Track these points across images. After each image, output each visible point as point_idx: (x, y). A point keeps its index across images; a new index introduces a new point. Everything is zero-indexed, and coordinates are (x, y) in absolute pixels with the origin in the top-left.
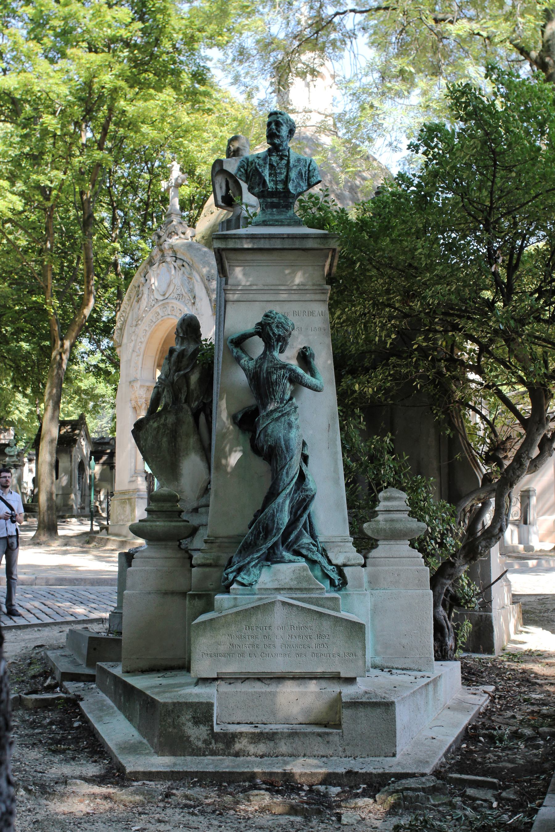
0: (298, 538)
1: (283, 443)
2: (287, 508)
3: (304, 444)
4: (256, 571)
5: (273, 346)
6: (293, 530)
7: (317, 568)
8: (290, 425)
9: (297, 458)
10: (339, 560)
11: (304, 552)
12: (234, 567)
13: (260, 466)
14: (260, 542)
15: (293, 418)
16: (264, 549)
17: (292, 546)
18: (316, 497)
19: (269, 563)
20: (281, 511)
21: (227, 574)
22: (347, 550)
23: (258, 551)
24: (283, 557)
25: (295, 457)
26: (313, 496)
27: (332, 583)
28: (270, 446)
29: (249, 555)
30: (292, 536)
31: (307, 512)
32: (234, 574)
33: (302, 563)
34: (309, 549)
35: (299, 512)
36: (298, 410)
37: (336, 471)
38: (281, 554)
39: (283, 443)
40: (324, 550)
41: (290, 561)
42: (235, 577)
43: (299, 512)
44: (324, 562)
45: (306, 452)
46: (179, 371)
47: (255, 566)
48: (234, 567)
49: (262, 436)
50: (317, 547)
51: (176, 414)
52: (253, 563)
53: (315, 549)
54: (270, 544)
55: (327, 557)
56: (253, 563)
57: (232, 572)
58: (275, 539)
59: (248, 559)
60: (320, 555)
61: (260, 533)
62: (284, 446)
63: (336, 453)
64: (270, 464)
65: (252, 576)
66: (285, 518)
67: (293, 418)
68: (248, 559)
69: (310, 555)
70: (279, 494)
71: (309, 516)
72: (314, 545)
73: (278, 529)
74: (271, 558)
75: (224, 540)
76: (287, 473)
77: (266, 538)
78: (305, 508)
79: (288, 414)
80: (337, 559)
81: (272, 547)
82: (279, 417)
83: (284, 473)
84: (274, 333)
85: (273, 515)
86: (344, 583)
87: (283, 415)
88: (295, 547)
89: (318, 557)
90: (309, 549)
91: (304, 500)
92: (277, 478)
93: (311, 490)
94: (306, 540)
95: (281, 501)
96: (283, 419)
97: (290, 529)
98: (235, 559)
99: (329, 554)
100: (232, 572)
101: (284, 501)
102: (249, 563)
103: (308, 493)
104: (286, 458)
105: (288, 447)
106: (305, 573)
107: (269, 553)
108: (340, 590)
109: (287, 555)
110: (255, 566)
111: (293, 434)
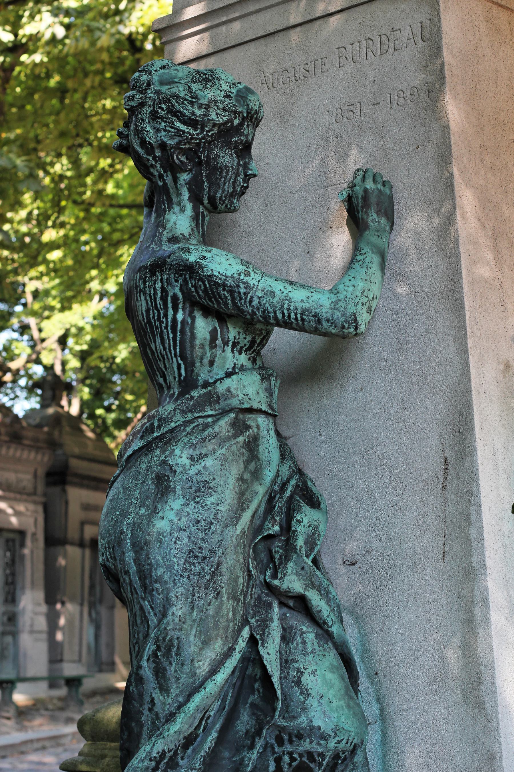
1: (129, 556)
5: (165, 189)
39: (129, 556)
67: (180, 456)
76: (160, 673)
84: (143, 143)
87: (147, 448)
103: (306, 745)
104: (146, 620)
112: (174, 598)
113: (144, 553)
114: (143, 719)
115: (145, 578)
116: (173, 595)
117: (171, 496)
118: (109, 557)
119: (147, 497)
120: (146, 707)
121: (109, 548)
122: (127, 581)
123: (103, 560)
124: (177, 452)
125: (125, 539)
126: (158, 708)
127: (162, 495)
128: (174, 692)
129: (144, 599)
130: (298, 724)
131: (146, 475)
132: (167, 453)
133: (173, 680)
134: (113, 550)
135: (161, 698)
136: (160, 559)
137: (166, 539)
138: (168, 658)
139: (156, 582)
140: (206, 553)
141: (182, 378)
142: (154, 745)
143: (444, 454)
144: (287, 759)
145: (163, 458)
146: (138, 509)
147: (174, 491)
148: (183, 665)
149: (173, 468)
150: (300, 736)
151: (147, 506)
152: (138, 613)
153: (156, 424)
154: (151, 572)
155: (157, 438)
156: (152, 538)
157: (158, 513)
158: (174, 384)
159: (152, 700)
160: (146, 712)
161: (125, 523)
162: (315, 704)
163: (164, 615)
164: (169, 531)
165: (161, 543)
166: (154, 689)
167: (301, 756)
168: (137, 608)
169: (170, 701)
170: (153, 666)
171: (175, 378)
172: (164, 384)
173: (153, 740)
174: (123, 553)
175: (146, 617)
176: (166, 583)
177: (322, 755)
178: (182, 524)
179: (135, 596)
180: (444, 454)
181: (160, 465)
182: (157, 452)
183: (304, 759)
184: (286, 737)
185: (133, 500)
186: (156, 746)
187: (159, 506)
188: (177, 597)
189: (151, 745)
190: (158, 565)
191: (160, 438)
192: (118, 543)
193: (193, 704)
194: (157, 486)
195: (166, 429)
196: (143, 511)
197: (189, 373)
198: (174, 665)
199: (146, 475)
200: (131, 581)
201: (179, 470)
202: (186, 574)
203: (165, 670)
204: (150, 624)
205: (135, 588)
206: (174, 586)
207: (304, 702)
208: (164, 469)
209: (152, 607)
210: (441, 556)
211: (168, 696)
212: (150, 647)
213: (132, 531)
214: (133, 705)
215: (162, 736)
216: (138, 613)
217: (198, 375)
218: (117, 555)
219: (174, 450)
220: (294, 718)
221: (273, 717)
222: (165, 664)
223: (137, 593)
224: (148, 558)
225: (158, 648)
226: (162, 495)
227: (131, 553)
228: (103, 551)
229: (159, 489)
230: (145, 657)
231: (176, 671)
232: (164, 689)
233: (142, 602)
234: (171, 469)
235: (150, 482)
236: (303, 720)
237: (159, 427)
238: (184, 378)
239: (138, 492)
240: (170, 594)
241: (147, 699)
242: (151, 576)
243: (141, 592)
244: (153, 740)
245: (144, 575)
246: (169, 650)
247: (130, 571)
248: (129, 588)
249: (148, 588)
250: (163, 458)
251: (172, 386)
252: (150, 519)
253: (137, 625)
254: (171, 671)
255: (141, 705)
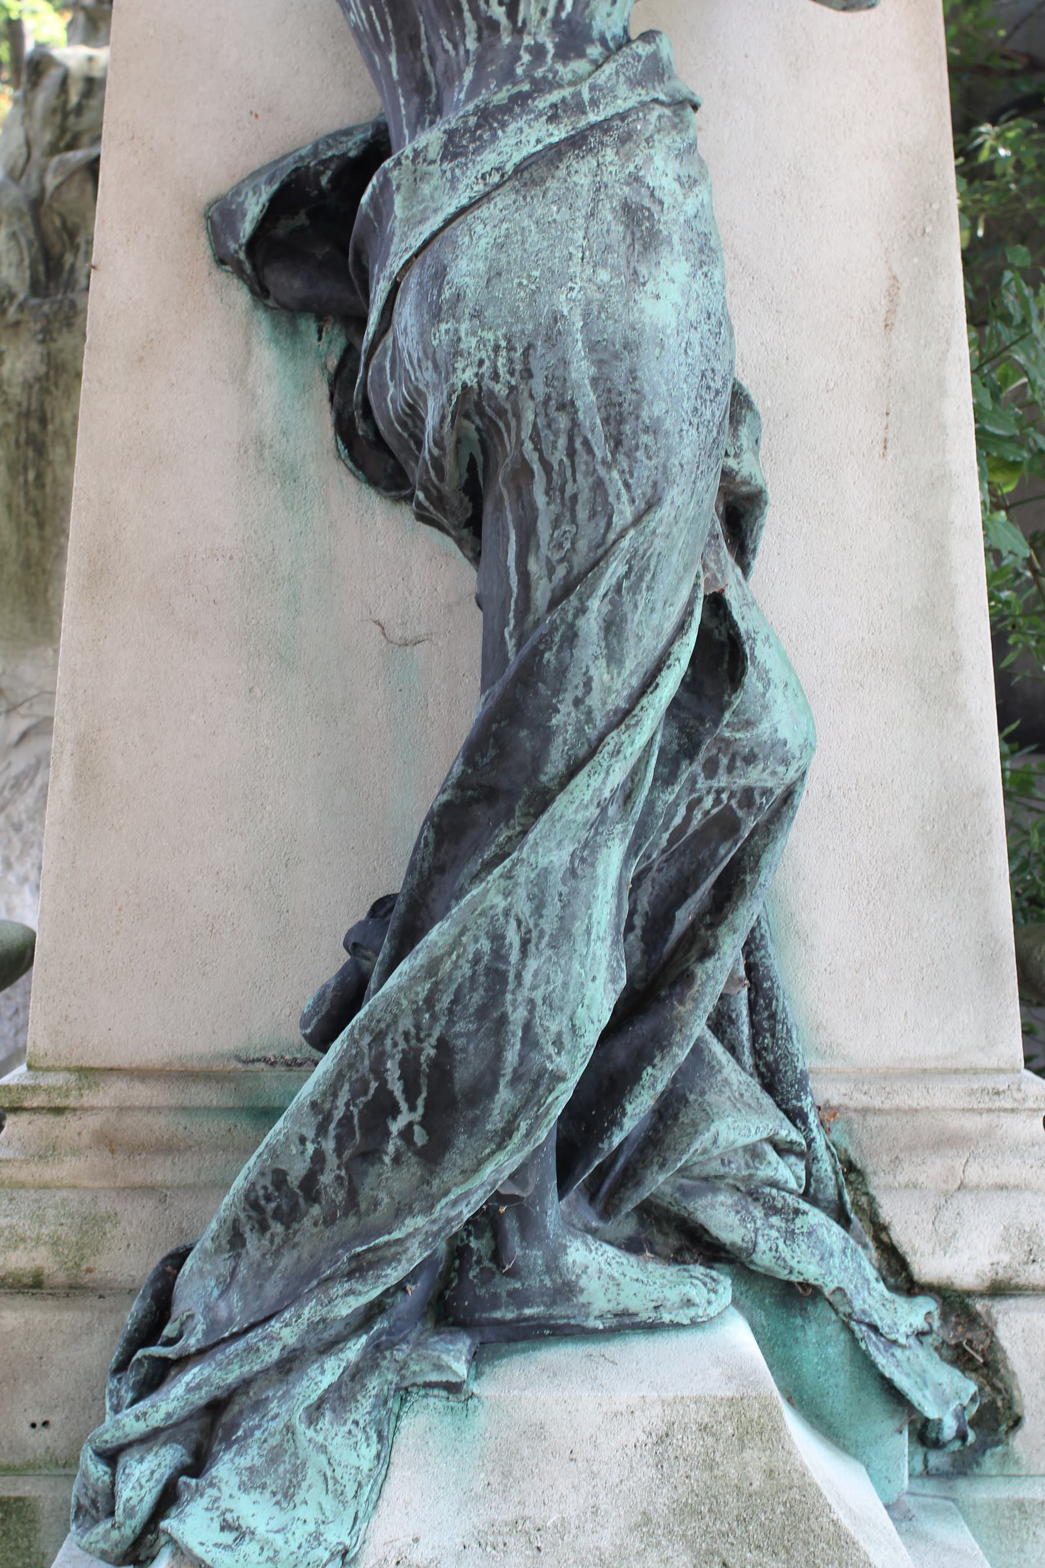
0: (669, 1109)
1: (581, 369)
2: (603, 907)
3: (740, 402)
4: (344, 1446)
6: (643, 1058)
7: (820, 1344)
8: (640, 223)
9: (688, 508)
10: (957, 1254)
11: (722, 1218)
12: (175, 1398)
13: (404, 569)
14: (390, 1180)
15: (661, 170)
16: (415, 1242)
17: (631, 1176)
18: (805, 803)
19: (455, 1358)
20: (563, 935)
21: (111, 1457)
22: (1011, 1170)
23: (360, 1269)
24: (566, 1290)
25: (675, 496)
26: (788, 796)
27: (924, 1434)
28: (471, 404)
29: (292, 1298)
30: (638, 1109)
31: (744, 916)
32: (165, 1459)
33: (727, 1344)
34: (753, 1193)
35: (684, 917)
36: (695, 118)
37: (934, 613)
38: (553, 1266)
39: (581, 369)
40: (851, 1170)
41: (625, 1325)
42: (168, 1499)
43: (684, 917)
44: (872, 1297)
45: (746, 467)
46: (71, 146)
47: (338, 1398)
48: (175, 1398)
49: (406, 314)
50: (807, 1155)
51: (46, 336)
52: (327, 1373)
53: (788, 1172)
54: (464, 1199)
55: (879, 1230)
56: (327, 1373)
57: (150, 1438)
58: (498, 1169)
59: (286, 1332)
60: (833, 1233)
61: (382, 1108)
62: (587, 399)
63: (939, 482)
64: (476, 558)
65: (313, 1495)
66: (593, 985)
68: (286, 1332)
69: (767, 1245)
70: (542, 801)
71: (752, 947)
72: (783, 1149)
73: (535, 1082)
74: (477, 1301)
75: (142, 1093)
76: (613, 626)
77: (432, 1155)
78: (730, 889)
79: (620, 131)
80: (946, 1243)
81: (487, 1220)
82: (553, 155)
83: (591, 625)
85: (496, 976)
86: (995, 1418)
87: (577, 142)
88: (658, 1182)
89: (826, 1255)
90: (753, 1193)
91: (724, 824)
92: (530, 673)
93: (778, 751)
94: (737, 1121)
95: (559, 858)
96: (581, 172)
97: (620, 1052)
98: (195, 1293)
99: (889, 1210)
100: (150, 1438)
101: (585, 856)
102: (289, 1365)
103: (755, 776)
105: (617, 417)
106: (754, 1457)
107: (459, 1251)
108: (965, 1464)
109: (599, 1268)
110: (338, 1398)
111: (666, 300)
112: (676, 470)
113: (623, 367)
114: (554, 721)
115: (621, 421)
116: (677, 463)
117: (664, 250)
118: (502, 371)
119: (608, 248)
120: (569, 697)
121: (511, 348)
122: (563, 422)
123: (477, 375)
124: (658, 161)
125: (569, 333)
126: (594, 700)
127: (646, 247)
128: (630, 665)
129: (607, 465)
130: (758, 736)
131: (596, 201)
132: (638, 161)
133: (632, 641)
134: (526, 354)
135: (606, 677)
136: (662, 382)
137: (671, 341)
138: (634, 594)
139: (646, 430)
140: (719, 384)
141: (564, 15)
142: (607, 773)
143: (890, 269)
144: (708, 802)
145: (631, 168)
146: (589, 271)
147: (670, 243)
148: (652, 610)
149: (656, 193)
150: (750, 759)
151: (613, 268)
152: (585, 496)
153: (586, 96)
154: (638, 406)
155: (592, 127)
156: (641, 335)
157: (644, 284)
158: (539, 25)
159: (588, 685)
160: (566, 707)
161: (563, 298)
162: (780, 699)
163: (652, 504)
164: (674, 325)
165: (663, 347)
166: (596, 658)
167: (732, 795)
168: (584, 484)
169: (618, 685)
170: (606, 608)
171: (544, 12)
172: (504, 21)
173: (605, 764)
174: (565, 363)
175: (606, 503)
176: (667, 434)
177: (766, 792)
178: (692, 315)
179: (582, 456)
180: (890, 269)
181: (628, 184)
182: (610, 154)
183: (734, 803)
184: (724, 761)
185: (571, 249)
186: (611, 777)
187: (643, 270)
188: (682, 466)
189: (603, 775)
190: (656, 394)
191: (603, 127)
192: (548, 338)
193: (667, 690)
194: (627, 226)
195: (610, 111)
196: (603, 275)
197: (580, 7)
198: (640, 609)
199: (596, 201)
200: (575, 423)
201: (668, 201)
202: (695, 421)
203: (624, 619)
204: (615, 519)
205: (586, 443)
206: (680, 443)
207: (764, 694)
208: (639, 193)
209: (627, 485)
210: (879, 448)
211: (619, 674)
212: (615, 569)
213: (586, 315)
214: (536, 693)
215: (621, 755)
216: (585, 496)
217: (592, 17)
218: (535, 365)
219: (650, 159)
220: (748, 724)
221: (716, 723)
222: (627, 607)
223: (590, 451)
224: (635, 379)
225: (627, 575)
226: (646, 247)
227: (584, 364)
228: (483, 355)
229: (633, 234)
230: (601, 591)
231: (640, 622)
232: (614, 658)
233: (602, 471)
234: (652, 195)
235: (610, 217)
236: (764, 728)
237: (594, 103)
238: (569, 15)
239: (581, 234)
240: (672, 460)
241: (575, 679)
242: (638, 418)
243: (601, 450)
244: (605, 764)
245: (621, 414)
246: (641, 578)
247: (578, 403)
248: (562, 442)
249: (625, 442)
250: (631, 168)
251: (531, 27)
252: (630, 297)
253: (573, 520)
254: (635, 620)
255: (557, 692)
